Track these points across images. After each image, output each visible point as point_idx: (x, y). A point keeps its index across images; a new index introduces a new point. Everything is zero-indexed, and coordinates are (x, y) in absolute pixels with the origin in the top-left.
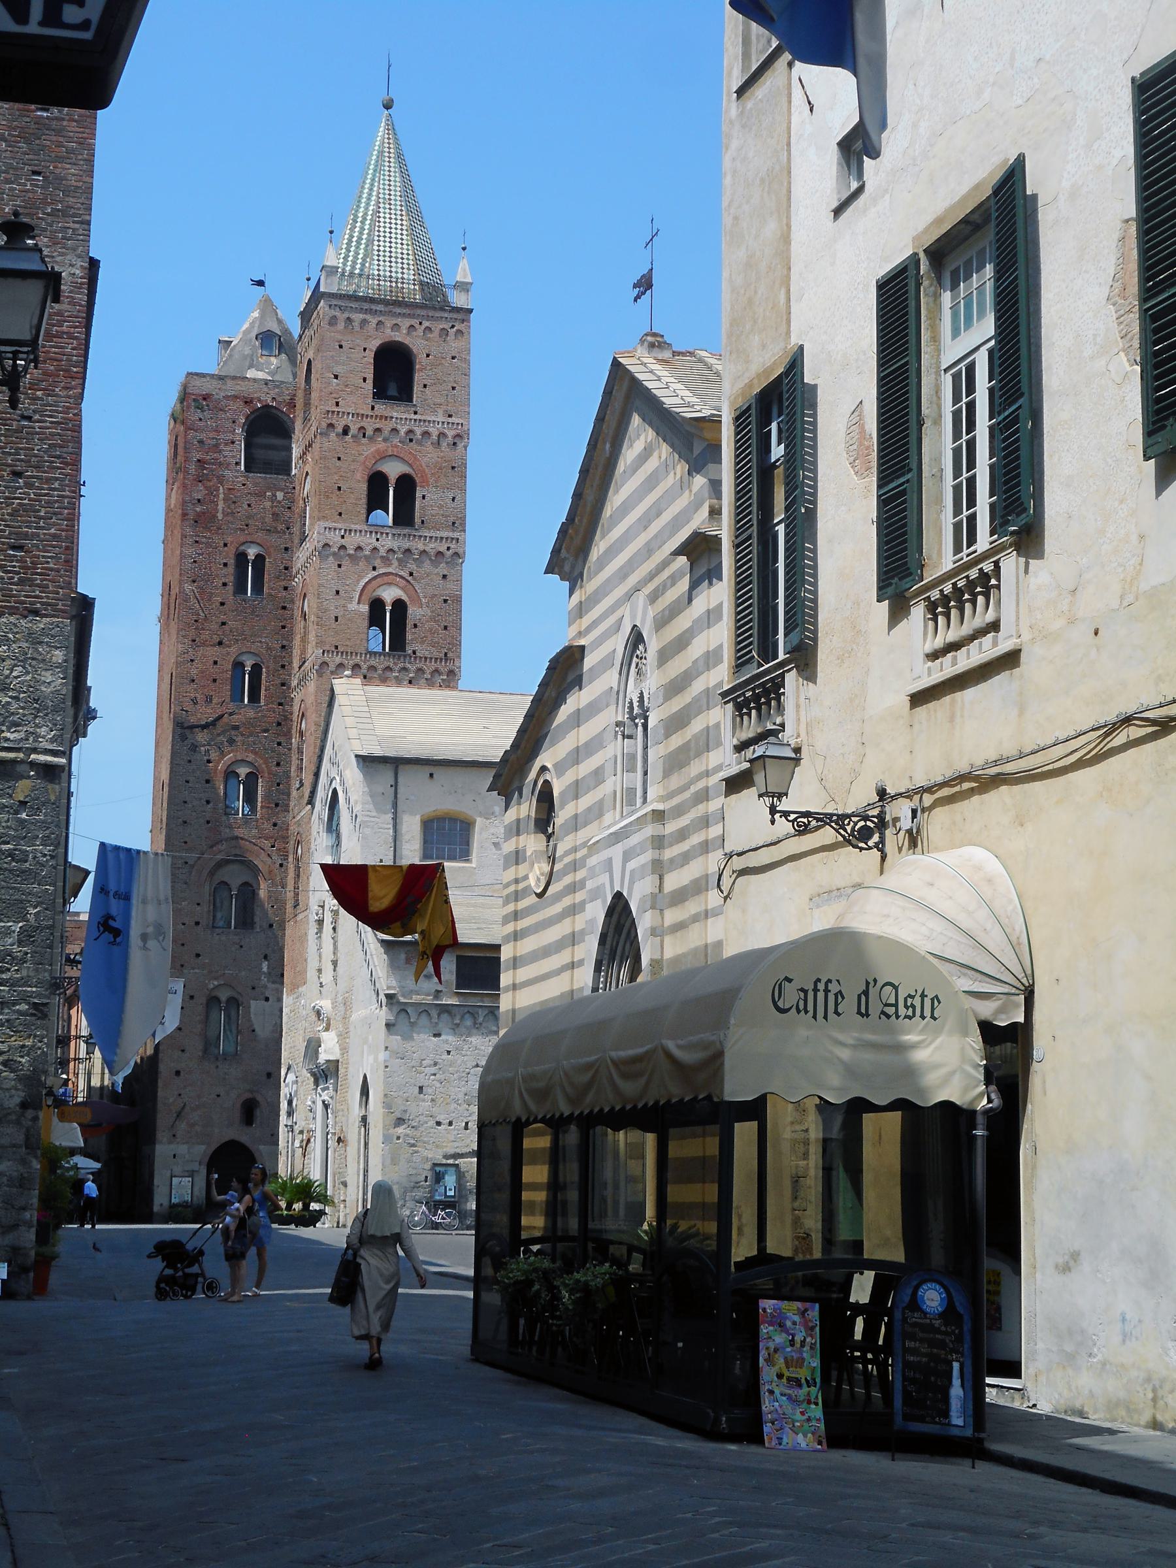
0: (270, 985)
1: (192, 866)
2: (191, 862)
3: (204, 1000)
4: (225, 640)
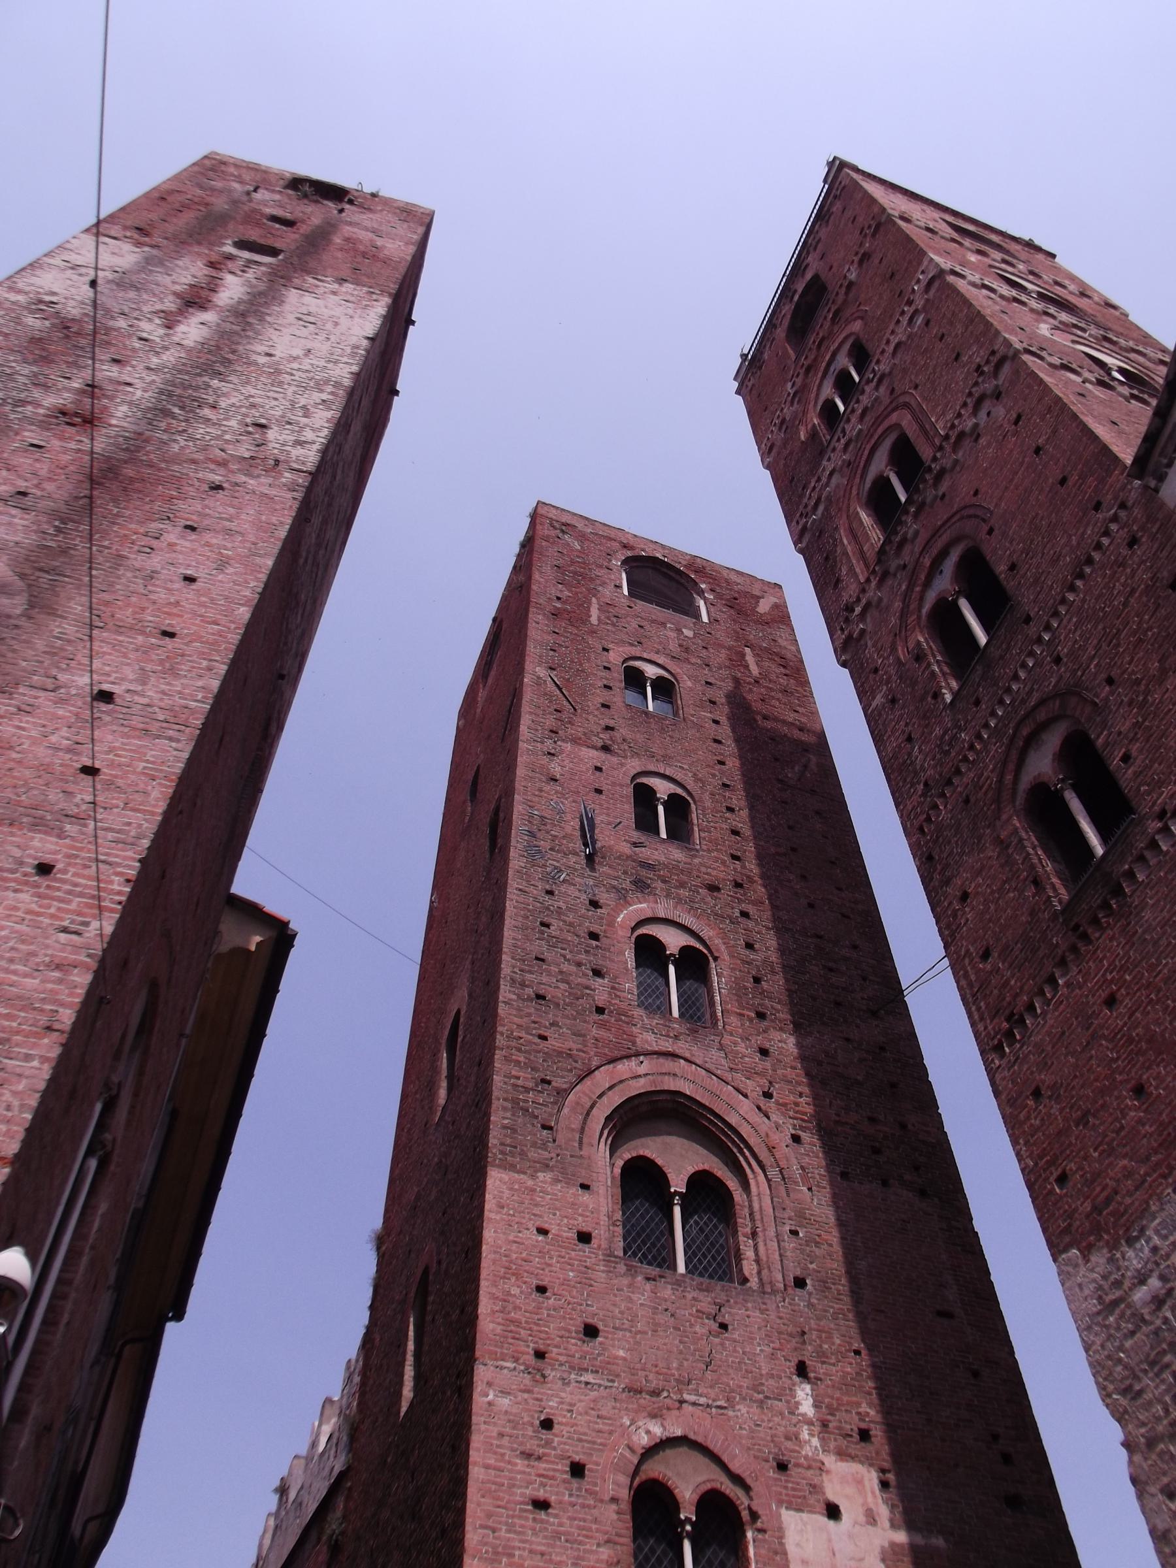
0: (830, 1461)
3: (615, 1484)
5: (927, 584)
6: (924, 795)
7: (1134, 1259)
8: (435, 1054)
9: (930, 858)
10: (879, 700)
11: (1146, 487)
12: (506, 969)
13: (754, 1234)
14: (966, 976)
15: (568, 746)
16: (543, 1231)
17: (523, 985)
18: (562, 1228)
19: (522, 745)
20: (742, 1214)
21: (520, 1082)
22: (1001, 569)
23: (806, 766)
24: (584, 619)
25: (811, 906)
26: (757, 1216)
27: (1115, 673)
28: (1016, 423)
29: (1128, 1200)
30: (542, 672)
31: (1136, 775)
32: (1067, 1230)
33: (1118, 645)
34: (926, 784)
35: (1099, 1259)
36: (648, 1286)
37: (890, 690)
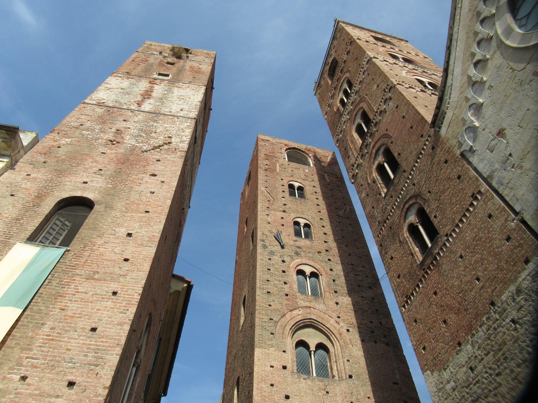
1: (276, 322)
2: (275, 319)
4: (287, 210)
5: (375, 158)
6: (378, 226)
7: (446, 375)
8: (240, 308)
9: (381, 245)
10: (363, 195)
11: (435, 131)
12: (258, 285)
13: (336, 362)
14: (394, 283)
15: (273, 212)
16: (272, 367)
17: (263, 289)
18: (278, 365)
19: (259, 213)
20: (332, 355)
21: (263, 320)
22: (396, 155)
23: (345, 210)
24: (275, 170)
25: (349, 255)
26: (337, 356)
27: (430, 190)
28: (397, 107)
29: (443, 356)
30: (263, 189)
31: (439, 222)
32: (426, 365)
33: (430, 181)
34: (379, 222)
35: (436, 374)
36: (304, 381)
37: (366, 192)
